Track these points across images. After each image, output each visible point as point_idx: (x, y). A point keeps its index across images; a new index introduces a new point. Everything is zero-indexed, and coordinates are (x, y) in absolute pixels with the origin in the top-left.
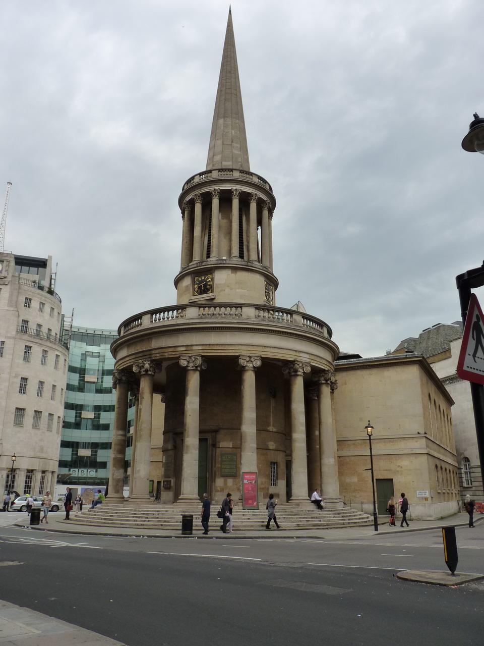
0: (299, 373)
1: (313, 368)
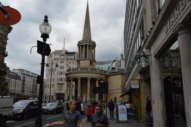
1: (91, 78)
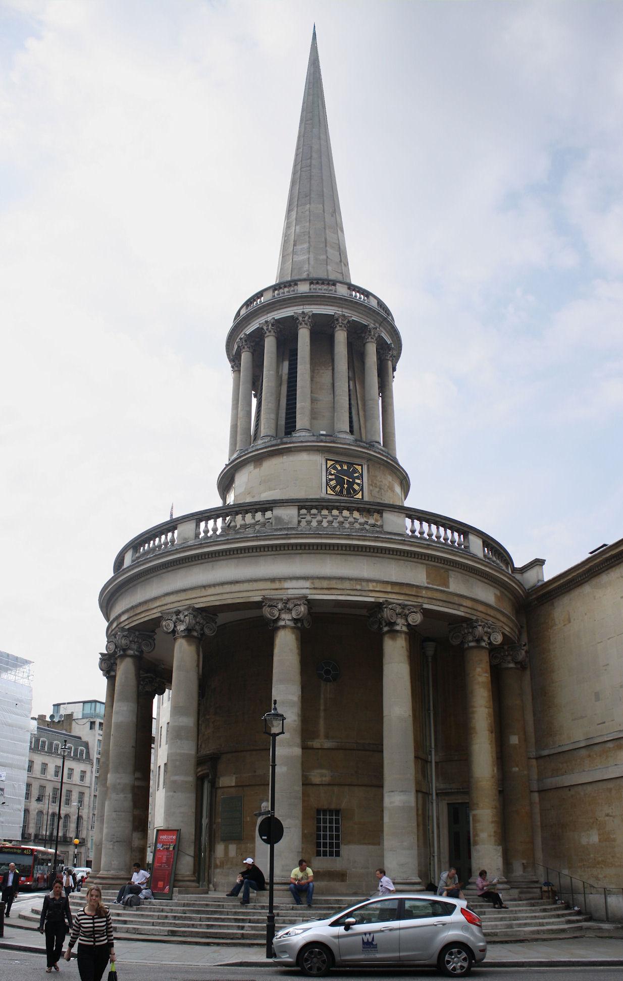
0: (282, 623)
1: (310, 603)
